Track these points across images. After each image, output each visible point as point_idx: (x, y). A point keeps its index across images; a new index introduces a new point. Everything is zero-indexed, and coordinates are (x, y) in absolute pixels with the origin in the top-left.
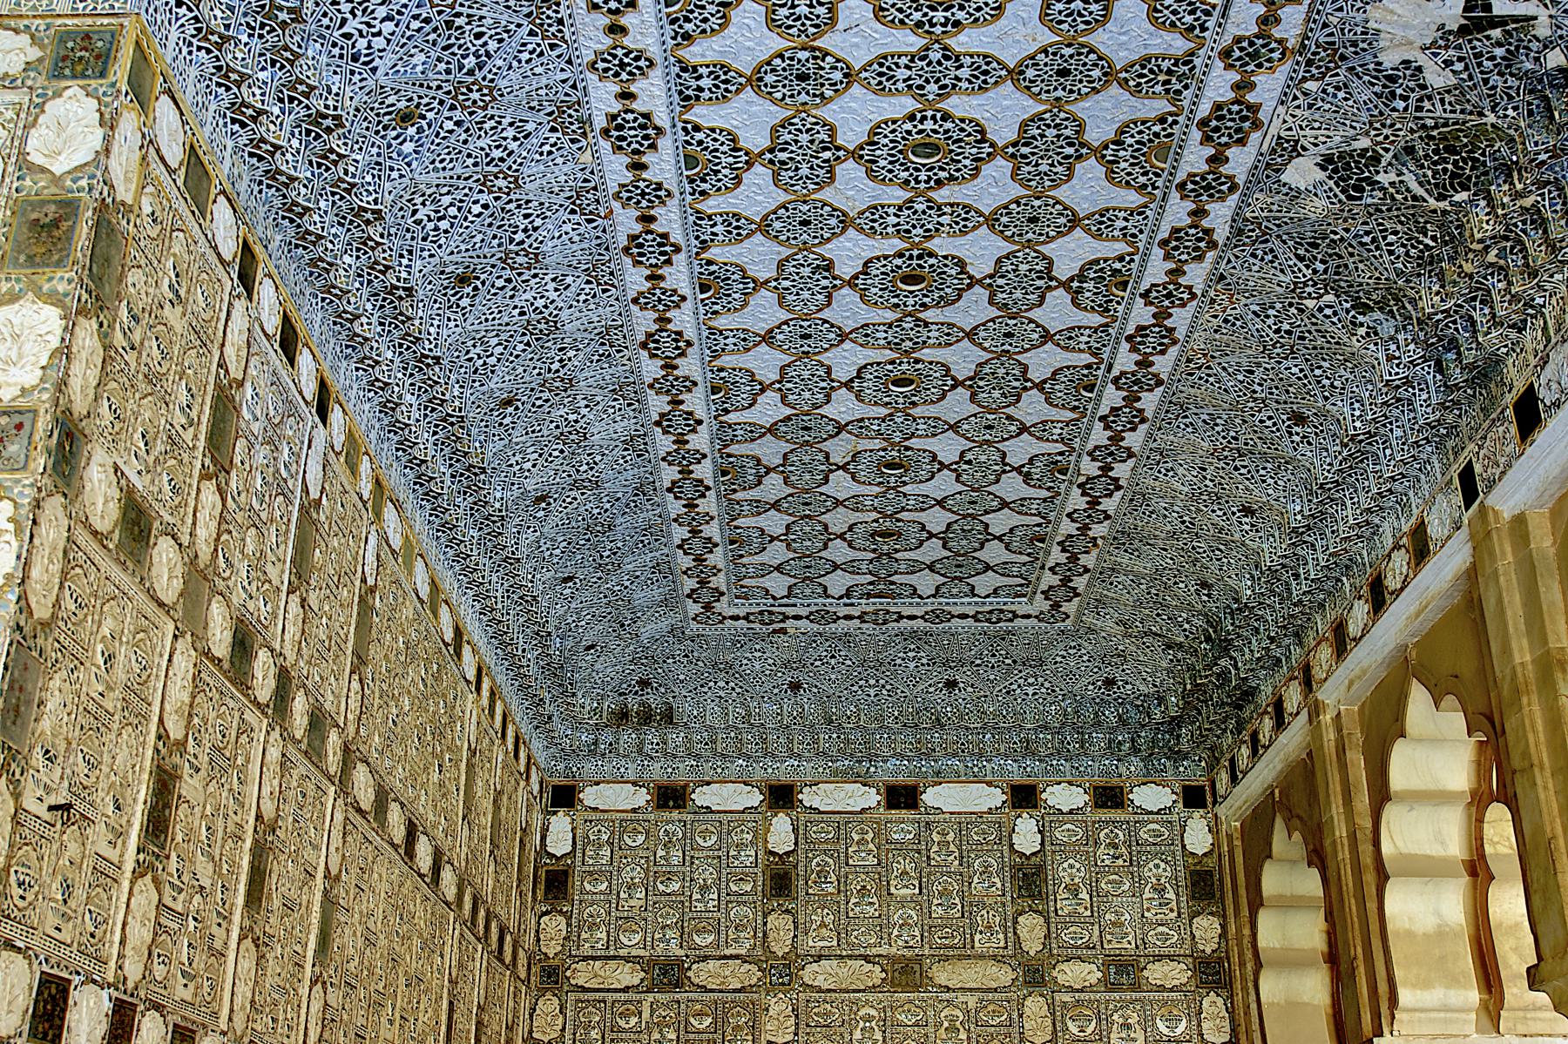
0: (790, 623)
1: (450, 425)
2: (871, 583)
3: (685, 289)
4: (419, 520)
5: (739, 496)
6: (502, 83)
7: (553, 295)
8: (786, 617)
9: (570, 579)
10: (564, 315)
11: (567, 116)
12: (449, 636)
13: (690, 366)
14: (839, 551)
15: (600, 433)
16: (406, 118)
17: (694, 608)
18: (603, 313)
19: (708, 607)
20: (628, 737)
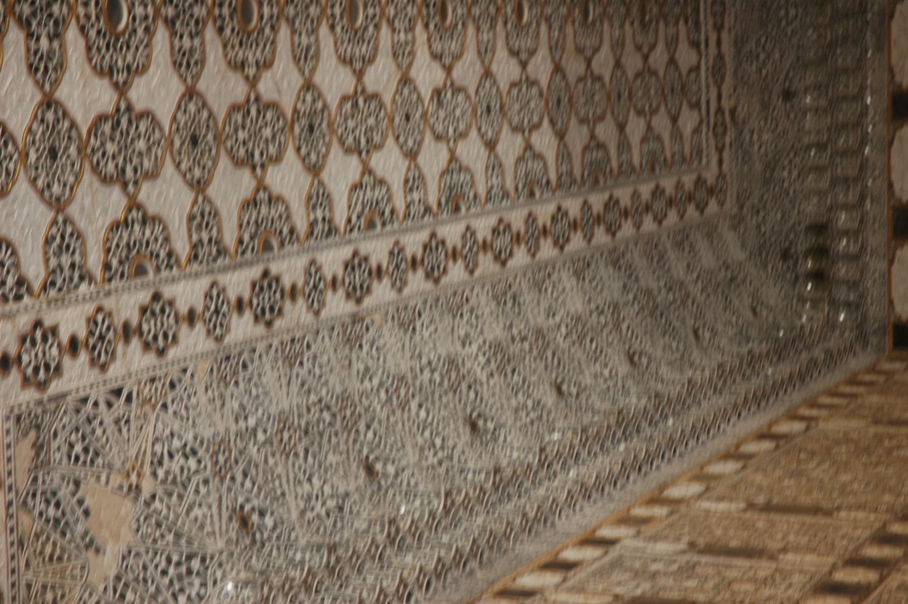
0: (726, 105)
1: (592, 440)
2: (686, 21)
3: (460, 227)
4: (676, 467)
5: (615, 164)
6: (338, 389)
7: (474, 347)
8: (720, 110)
9: (696, 332)
10: (490, 337)
11: (352, 333)
12: (767, 445)
13: (517, 219)
14: (659, 58)
15: (576, 304)
16: (370, 470)
17: (712, 207)
18: (483, 301)
19: (711, 191)
20: (842, 270)
